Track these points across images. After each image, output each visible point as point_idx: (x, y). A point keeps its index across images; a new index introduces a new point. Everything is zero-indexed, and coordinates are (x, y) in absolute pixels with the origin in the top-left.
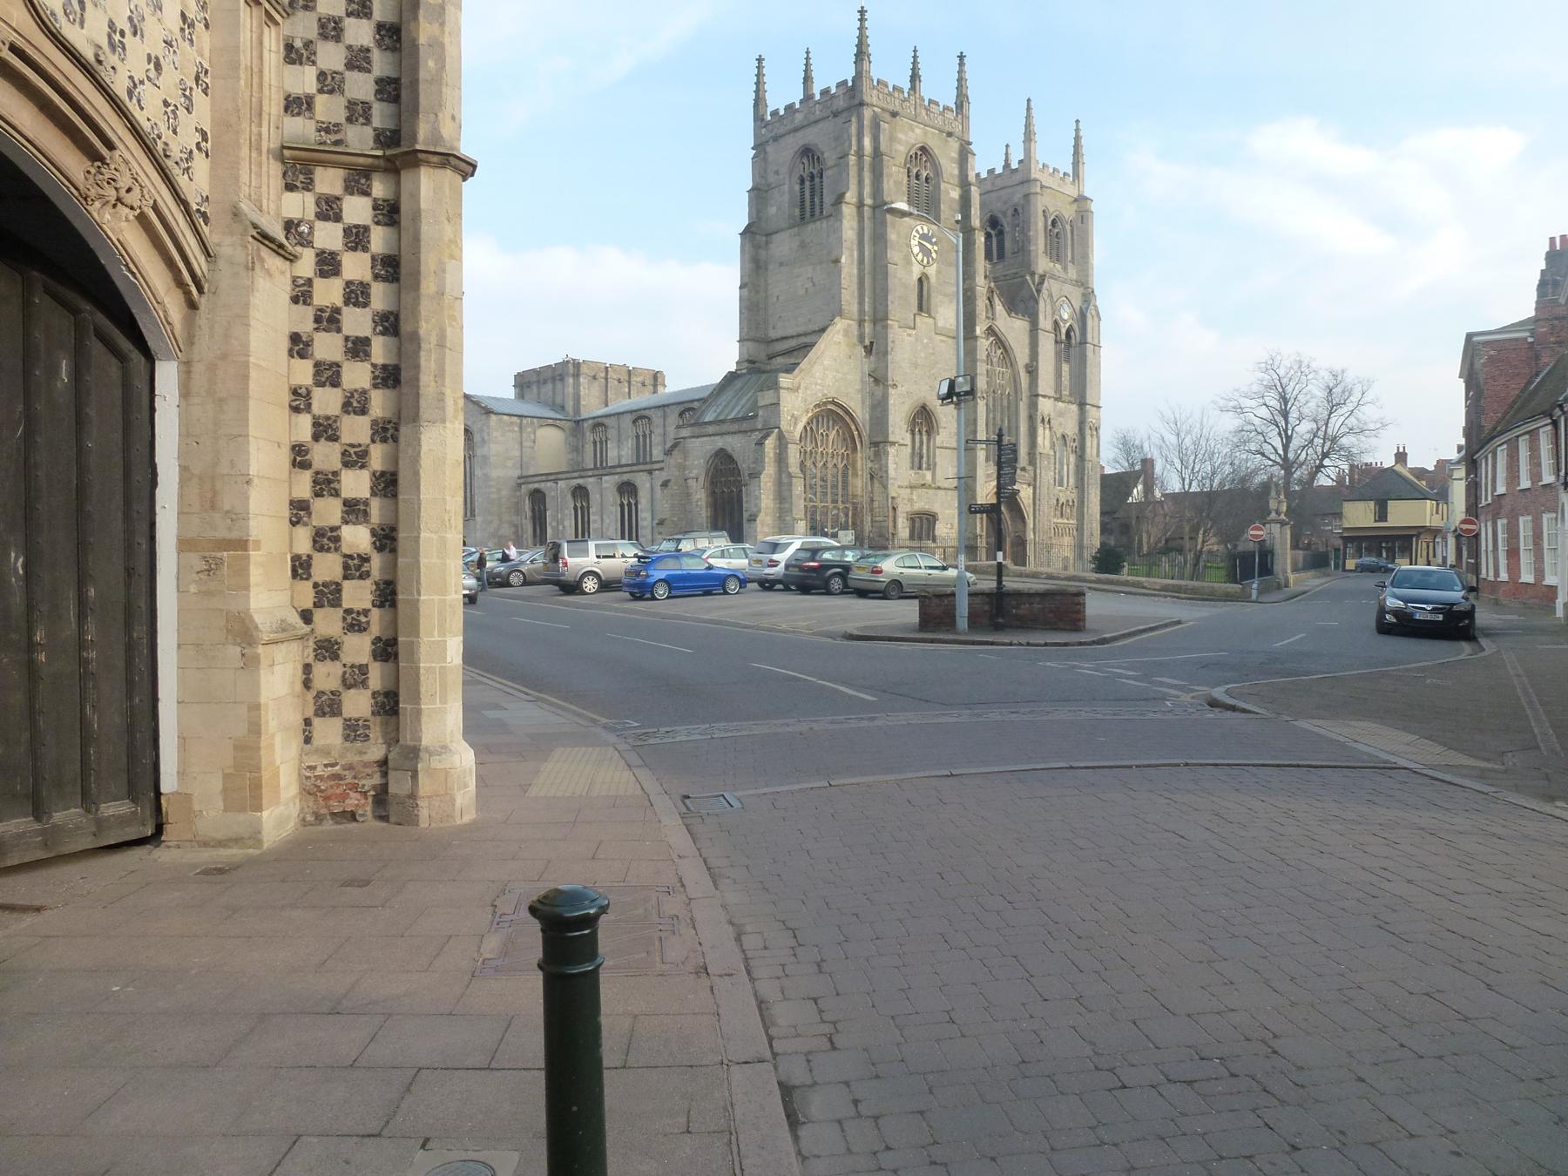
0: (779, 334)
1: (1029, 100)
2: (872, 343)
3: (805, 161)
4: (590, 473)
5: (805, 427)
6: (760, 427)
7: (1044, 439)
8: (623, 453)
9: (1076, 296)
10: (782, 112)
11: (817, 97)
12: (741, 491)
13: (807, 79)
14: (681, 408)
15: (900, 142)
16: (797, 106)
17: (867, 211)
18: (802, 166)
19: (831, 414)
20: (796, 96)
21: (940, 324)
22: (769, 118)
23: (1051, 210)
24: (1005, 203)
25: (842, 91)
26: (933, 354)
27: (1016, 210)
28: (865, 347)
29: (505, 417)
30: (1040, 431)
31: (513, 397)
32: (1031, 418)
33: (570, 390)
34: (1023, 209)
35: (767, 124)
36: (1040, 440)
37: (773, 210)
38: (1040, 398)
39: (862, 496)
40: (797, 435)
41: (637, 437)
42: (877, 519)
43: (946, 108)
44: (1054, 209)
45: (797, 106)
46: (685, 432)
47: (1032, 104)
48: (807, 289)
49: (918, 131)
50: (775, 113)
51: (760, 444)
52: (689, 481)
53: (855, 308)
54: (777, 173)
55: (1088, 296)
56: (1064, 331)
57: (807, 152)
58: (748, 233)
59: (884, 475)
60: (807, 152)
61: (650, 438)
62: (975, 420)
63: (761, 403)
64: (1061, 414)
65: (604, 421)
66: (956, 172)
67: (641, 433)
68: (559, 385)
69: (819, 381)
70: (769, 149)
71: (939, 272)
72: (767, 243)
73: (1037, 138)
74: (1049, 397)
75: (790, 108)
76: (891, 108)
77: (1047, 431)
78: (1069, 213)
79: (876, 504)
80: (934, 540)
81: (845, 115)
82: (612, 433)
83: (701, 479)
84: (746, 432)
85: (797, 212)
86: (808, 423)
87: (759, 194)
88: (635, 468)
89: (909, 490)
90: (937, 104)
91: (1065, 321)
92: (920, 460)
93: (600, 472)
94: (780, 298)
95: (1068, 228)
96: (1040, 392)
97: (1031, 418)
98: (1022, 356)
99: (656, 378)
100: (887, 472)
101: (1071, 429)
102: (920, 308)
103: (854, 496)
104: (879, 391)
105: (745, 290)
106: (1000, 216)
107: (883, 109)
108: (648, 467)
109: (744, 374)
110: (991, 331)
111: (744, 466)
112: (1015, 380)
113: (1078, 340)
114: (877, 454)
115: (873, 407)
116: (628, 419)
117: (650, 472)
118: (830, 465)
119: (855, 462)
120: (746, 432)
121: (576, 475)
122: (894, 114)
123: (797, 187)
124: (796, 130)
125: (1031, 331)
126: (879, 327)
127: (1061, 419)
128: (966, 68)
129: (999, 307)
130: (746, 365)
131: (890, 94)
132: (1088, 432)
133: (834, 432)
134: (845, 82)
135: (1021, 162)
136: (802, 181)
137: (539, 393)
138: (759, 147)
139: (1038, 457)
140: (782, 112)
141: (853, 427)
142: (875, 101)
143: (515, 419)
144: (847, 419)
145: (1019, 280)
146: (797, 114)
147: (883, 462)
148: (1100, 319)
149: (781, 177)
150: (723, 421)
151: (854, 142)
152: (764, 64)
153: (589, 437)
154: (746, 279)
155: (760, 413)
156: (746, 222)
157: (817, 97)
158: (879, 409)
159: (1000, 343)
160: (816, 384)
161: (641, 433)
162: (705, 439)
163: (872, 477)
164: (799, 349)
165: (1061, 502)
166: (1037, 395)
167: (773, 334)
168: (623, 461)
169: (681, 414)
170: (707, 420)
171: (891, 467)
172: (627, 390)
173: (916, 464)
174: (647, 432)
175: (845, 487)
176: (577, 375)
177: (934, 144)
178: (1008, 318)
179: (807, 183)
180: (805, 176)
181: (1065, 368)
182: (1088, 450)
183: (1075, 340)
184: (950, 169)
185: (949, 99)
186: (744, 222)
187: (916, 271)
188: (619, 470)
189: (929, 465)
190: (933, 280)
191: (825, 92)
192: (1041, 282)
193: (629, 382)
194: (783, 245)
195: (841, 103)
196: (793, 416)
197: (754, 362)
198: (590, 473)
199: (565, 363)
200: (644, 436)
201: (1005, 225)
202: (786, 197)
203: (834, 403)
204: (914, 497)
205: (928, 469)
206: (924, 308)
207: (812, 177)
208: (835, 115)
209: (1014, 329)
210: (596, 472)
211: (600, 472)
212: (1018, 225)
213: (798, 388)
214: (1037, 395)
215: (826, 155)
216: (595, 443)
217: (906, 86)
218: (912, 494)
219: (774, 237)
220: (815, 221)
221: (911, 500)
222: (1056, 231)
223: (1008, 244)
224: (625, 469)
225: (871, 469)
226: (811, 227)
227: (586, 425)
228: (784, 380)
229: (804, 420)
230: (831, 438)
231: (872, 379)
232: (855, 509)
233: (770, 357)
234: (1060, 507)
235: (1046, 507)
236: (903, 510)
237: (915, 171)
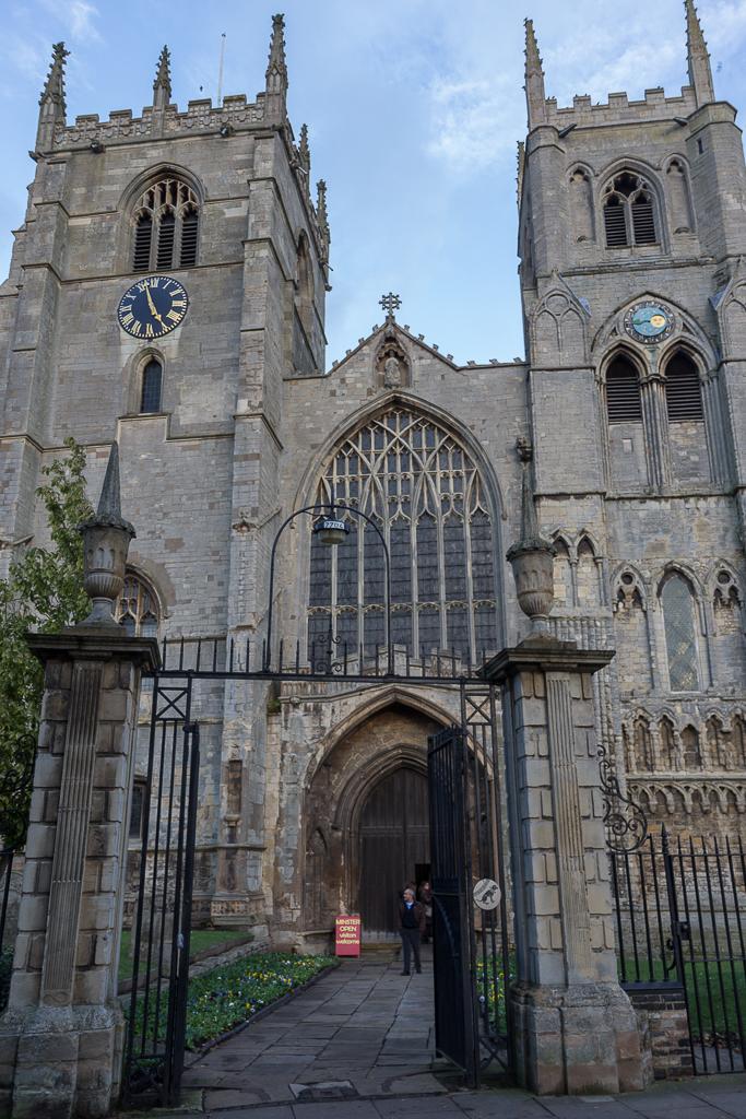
1: (528, 23)
15: (111, 180)
21: (183, 421)
26: (163, 474)
71: (184, 338)
77: (586, 570)
78: (653, 150)
91: (652, 340)
166: (537, 498)
177: (190, 157)
183: (705, 360)
187: (130, 347)
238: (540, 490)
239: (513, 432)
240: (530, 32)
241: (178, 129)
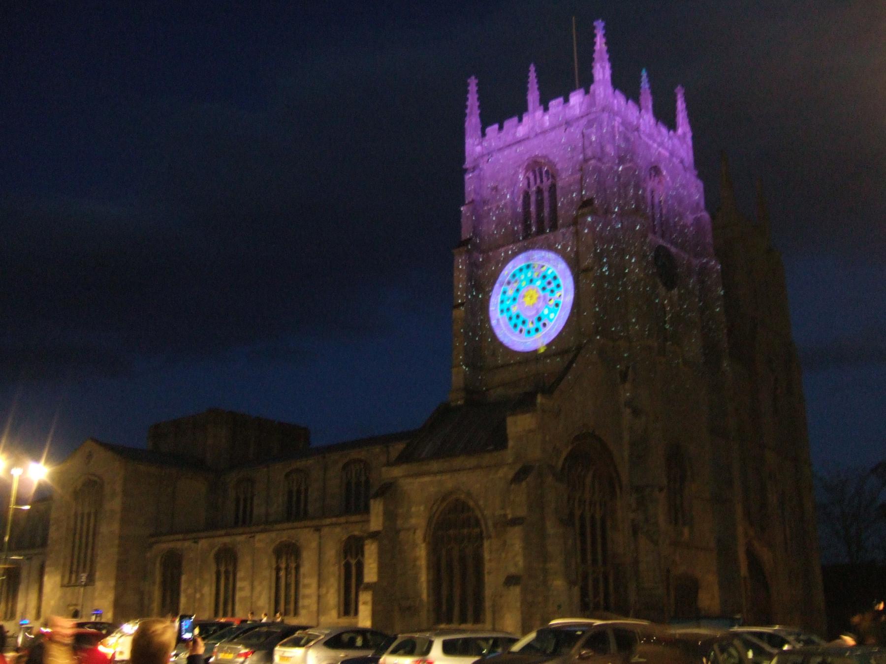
41: (290, 493)
86: (566, 459)
133: (590, 474)
161: (295, 489)
162: (426, 479)
163: (635, 530)
200: (299, 492)
216: (238, 500)
230: (588, 480)
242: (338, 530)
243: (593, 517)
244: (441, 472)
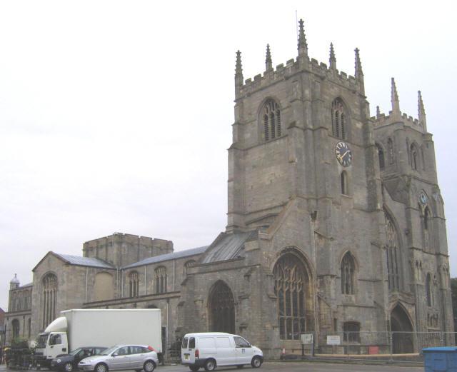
0: (253, 210)
1: (393, 79)
2: (316, 212)
3: (268, 106)
4: (128, 301)
5: (276, 266)
6: (246, 265)
7: (419, 277)
8: (148, 289)
9: (429, 189)
10: (253, 80)
11: (275, 70)
12: (233, 308)
13: (269, 61)
14: (187, 260)
16: (262, 76)
17: (310, 133)
18: (265, 109)
19: (292, 258)
20: (261, 70)
21: (356, 201)
22: (244, 84)
23: (410, 139)
24: (383, 135)
25: (291, 65)
27: (390, 139)
28: (312, 215)
29: (77, 268)
30: (416, 271)
31: (82, 255)
32: (410, 262)
33: (115, 251)
34: (394, 137)
35: (243, 87)
36: (416, 276)
37: (248, 136)
38: (415, 250)
39: (313, 312)
40: (272, 269)
41: (158, 279)
42: (324, 326)
43: (351, 77)
44: (412, 137)
45: (262, 76)
46: (195, 270)
47: (395, 80)
48: (271, 181)
49: (336, 89)
50: (248, 81)
51: (247, 276)
52: (198, 302)
53: (304, 190)
54: (250, 114)
55: (436, 189)
56: (423, 210)
57: (270, 101)
58: (233, 149)
59: (327, 297)
60: (270, 101)
61: (166, 278)
62: (381, 262)
63: (247, 249)
64: (426, 260)
65: (138, 270)
66: (359, 113)
67: (160, 277)
68: (109, 248)
69: (285, 236)
70: (245, 101)
72: (245, 155)
73: (399, 98)
74: (420, 250)
75: (258, 77)
76: (320, 74)
77: (420, 271)
78: (419, 142)
79: (323, 316)
80: (359, 341)
81: (292, 79)
82: (143, 277)
83: (206, 301)
84: (236, 268)
85: (263, 136)
87: (239, 126)
88: (157, 297)
89: (342, 308)
90: (345, 74)
91: (424, 204)
92: (347, 288)
93: (135, 300)
94: (254, 187)
95: (420, 151)
96: (414, 246)
97: (410, 262)
98: (401, 223)
99: (168, 246)
100: (329, 295)
101: (431, 268)
102: (343, 193)
103: (308, 311)
104: (322, 243)
105: (232, 183)
106: (381, 143)
107: (316, 75)
108: (166, 296)
109: (232, 234)
110: (384, 208)
111: (236, 292)
112: (399, 239)
113: (432, 216)
114: (322, 284)
115: (319, 253)
116: (152, 268)
117: (168, 299)
118: (292, 290)
119: (308, 288)
120: (236, 268)
121: (119, 302)
122: (322, 78)
123: (263, 122)
124: (262, 89)
125: (406, 209)
126: (320, 202)
127: (426, 263)
128: (360, 56)
129: (387, 194)
130: (232, 228)
131: (319, 67)
132: (442, 272)
133: (294, 269)
134: (293, 60)
135: (390, 112)
136: (266, 118)
137: (97, 254)
138: (239, 100)
139: (416, 286)
140: (253, 80)
141: (306, 266)
142: (311, 70)
143: (83, 268)
144: (302, 260)
145: (395, 179)
146: (262, 81)
147: (327, 288)
148: (443, 203)
149: (253, 116)
150: (222, 262)
151: (300, 92)
152: (241, 55)
153: (128, 279)
154: (232, 176)
155: (247, 256)
156: (231, 143)
157: (275, 70)
158: (323, 252)
159: (388, 215)
160: (283, 237)
161: (160, 277)
163: (319, 299)
164: (269, 219)
165: (430, 316)
167: (249, 209)
168: (148, 294)
169: (185, 265)
170: (208, 262)
171: (333, 292)
172: (150, 252)
173: (345, 290)
174: (164, 276)
175: (301, 304)
176: (120, 243)
177: (344, 95)
178: (393, 202)
179: (269, 119)
180: (268, 115)
181: (426, 232)
182: (444, 282)
184: (356, 111)
185: (351, 72)
186: (229, 142)
187: (340, 168)
188: (147, 298)
189: (352, 291)
190: (350, 175)
191: (280, 67)
192: (410, 180)
193: (152, 247)
194: (256, 156)
195: (290, 72)
196: (268, 257)
197: (236, 227)
198: (128, 301)
199: (115, 235)
200: (162, 278)
201: (384, 147)
202: (256, 128)
203: (293, 249)
204: (346, 312)
205: (352, 294)
206: (345, 191)
207: (272, 115)
208: (287, 78)
209: (396, 208)
210: (132, 300)
211: (135, 300)
212: (392, 148)
213: (271, 239)
214: (413, 248)
215: (281, 102)
216: (131, 283)
217: (328, 66)
218: (344, 310)
219: (250, 152)
220: (275, 140)
221: (344, 314)
222: (414, 151)
223: (386, 159)
224: (152, 298)
225: (318, 293)
226: (273, 144)
227: (126, 272)
228: (262, 234)
229: (276, 261)
231: (316, 235)
232: (309, 320)
233: (248, 224)
234: (432, 319)
235: (423, 320)
236: (341, 320)
237: (335, 111)
238: (414, 245)
239: (405, 227)
240: (393, 83)
241: (340, 82)
242: (177, 299)
243: (295, 291)
244: (216, 271)
